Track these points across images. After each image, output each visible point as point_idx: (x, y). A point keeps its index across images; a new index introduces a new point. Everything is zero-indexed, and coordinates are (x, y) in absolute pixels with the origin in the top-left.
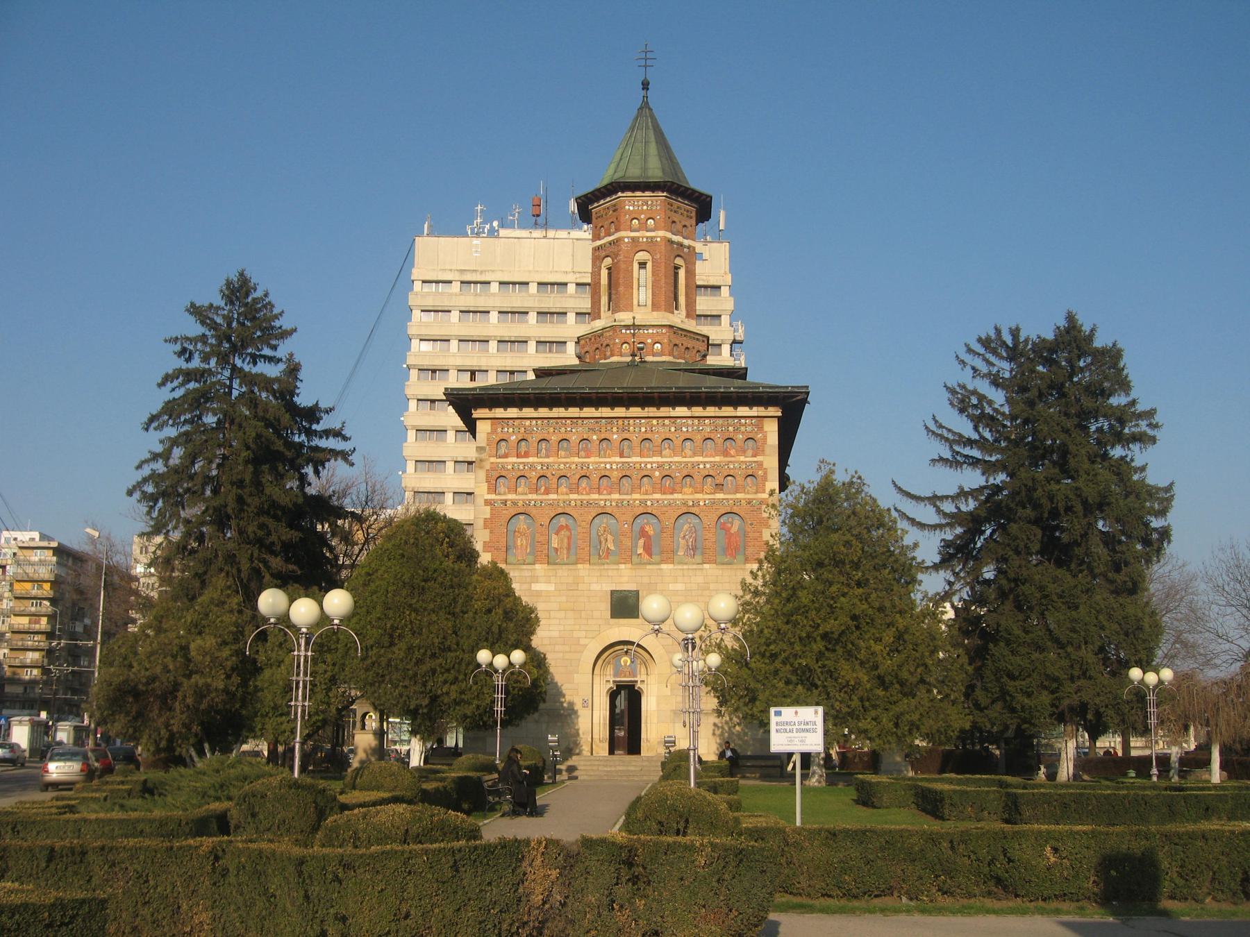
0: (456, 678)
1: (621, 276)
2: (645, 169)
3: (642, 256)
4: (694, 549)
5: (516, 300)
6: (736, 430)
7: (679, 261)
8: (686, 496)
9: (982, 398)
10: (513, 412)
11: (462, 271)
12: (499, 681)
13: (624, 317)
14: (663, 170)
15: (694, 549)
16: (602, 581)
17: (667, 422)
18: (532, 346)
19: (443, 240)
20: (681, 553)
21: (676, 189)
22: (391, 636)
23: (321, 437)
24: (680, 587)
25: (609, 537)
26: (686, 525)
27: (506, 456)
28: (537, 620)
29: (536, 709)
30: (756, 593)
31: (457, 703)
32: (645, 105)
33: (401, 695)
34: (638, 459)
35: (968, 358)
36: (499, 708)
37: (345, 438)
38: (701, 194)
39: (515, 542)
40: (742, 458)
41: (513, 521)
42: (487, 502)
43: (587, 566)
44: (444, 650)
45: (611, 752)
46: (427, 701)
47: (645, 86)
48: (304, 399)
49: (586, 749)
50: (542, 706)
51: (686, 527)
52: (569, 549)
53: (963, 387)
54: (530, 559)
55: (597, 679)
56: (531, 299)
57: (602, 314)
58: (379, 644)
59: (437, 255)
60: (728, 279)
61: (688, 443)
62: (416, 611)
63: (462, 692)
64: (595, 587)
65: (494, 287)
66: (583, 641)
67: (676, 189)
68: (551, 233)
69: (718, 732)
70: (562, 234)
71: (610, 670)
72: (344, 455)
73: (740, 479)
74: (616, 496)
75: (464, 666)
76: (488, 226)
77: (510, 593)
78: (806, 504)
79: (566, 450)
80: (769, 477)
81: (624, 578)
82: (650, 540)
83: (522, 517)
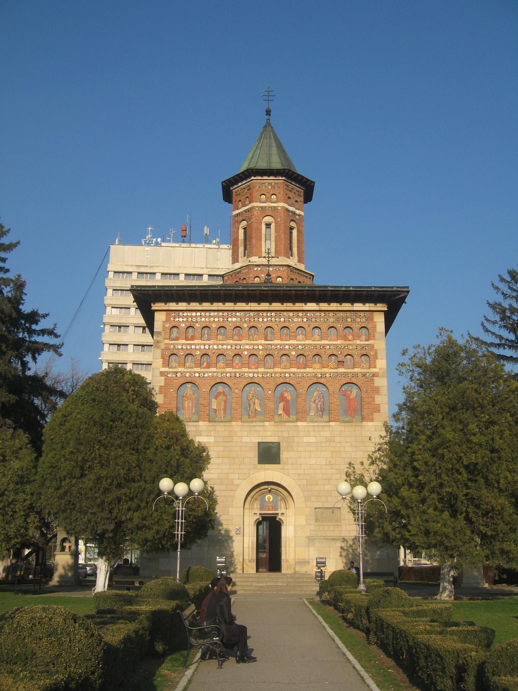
0: (139, 507)
1: (254, 232)
2: (269, 162)
3: (268, 219)
4: (322, 410)
6: (353, 321)
7: (293, 224)
8: (315, 370)
10: (183, 306)
11: (138, 266)
12: (180, 507)
13: (255, 260)
14: (282, 164)
15: (322, 410)
17: (300, 314)
20: (312, 413)
21: (290, 175)
22: (82, 468)
23: (39, 335)
24: (312, 439)
25: (257, 401)
26: (317, 392)
27: (177, 339)
28: (208, 458)
29: (205, 535)
31: (139, 528)
32: (268, 125)
33: (89, 521)
34: (279, 342)
36: (179, 532)
37: (57, 336)
38: (308, 180)
39: (183, 405)
40: (358, 342)
41: (182, 388)
42: (162, 374)
43: (240, 423)
44: (129, 481)
45: (257, 571)
46: (112, 527)
47: (268, 112)
48: (26, 308)
49: (239, 567)
50: (210, 532)
51: (316, 394)
52: (225, 410)
54: (195, 417)
55: (247, 511)
57: (240, 259)
58: (71, 475)
61: (317, 331)
62: (105, 446)
63: (144, 519)
64: (245, 439)
66: (236, 482)
67: (290, 175)
68: (193, 245)
69: (344, 554)
72: (55, 348)
74: (262, 370)
75: (145, 495)
76: (155, 240)
77: (184, 434)
78: (433, 361)
79: (223, 335)
80: (379, 355)
81: (269, 432)
82: (289, 403)
83: (189, 385)
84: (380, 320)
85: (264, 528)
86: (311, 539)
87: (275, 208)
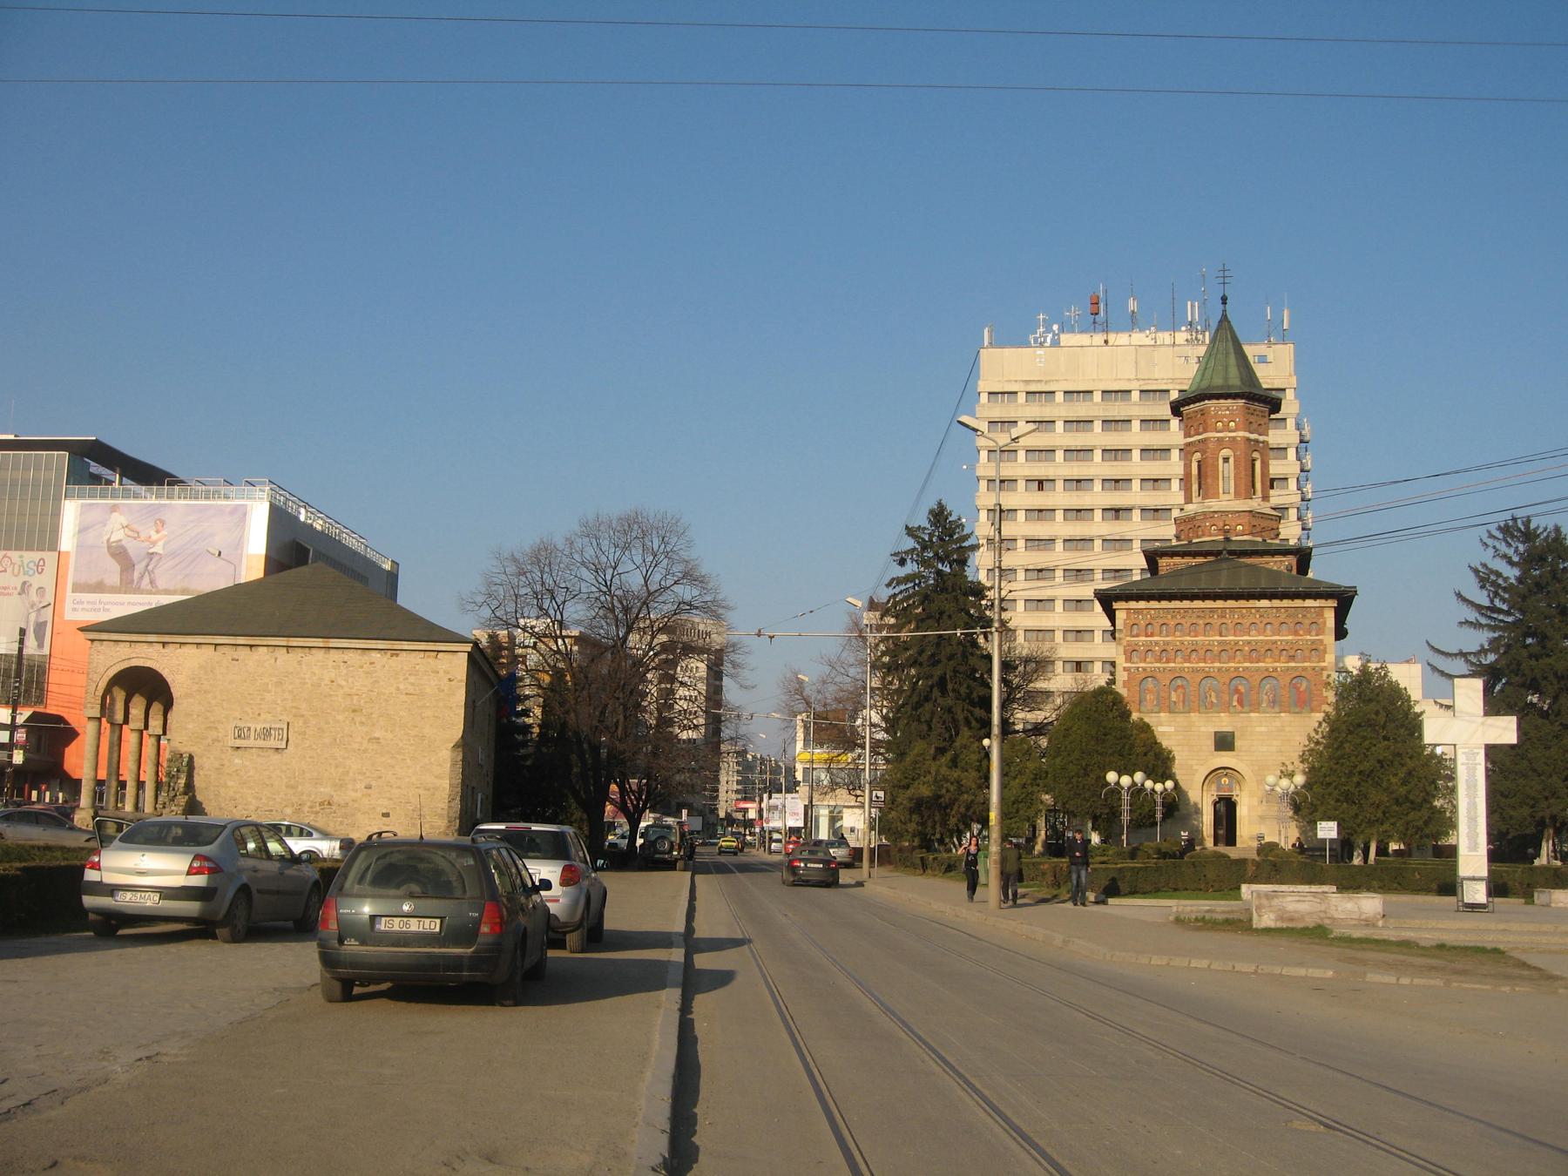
2: (1226, 379)
3: (1225, 452)
5: (1080, 410)
7: (1256, 455)
9: (1499, 574)
10: (1142, 604)
11: (1027, 382)
12: (1159, 800)
13: (1214, 505)
16: (1208, 725)
18: (1098, 455)
19: (1007, 351)
30: (1318, 743)
32: (1224, 318)
35: (1490, 542)
36: (1159, 816)
42: (1125, 669)
47: (1224, 300)
53: (1484, 565)
56: (1095, 408)
59: (1003, 366)
60: (1294, 381)
65: (1059, 397)
68: (1112, 337)
71: (1214, 787)
73: (1307, 653)
81: (1224, 723)
82: (1242, 697)
84: (1330, 618)
85: (1223, 809)
86: (1262, 818)
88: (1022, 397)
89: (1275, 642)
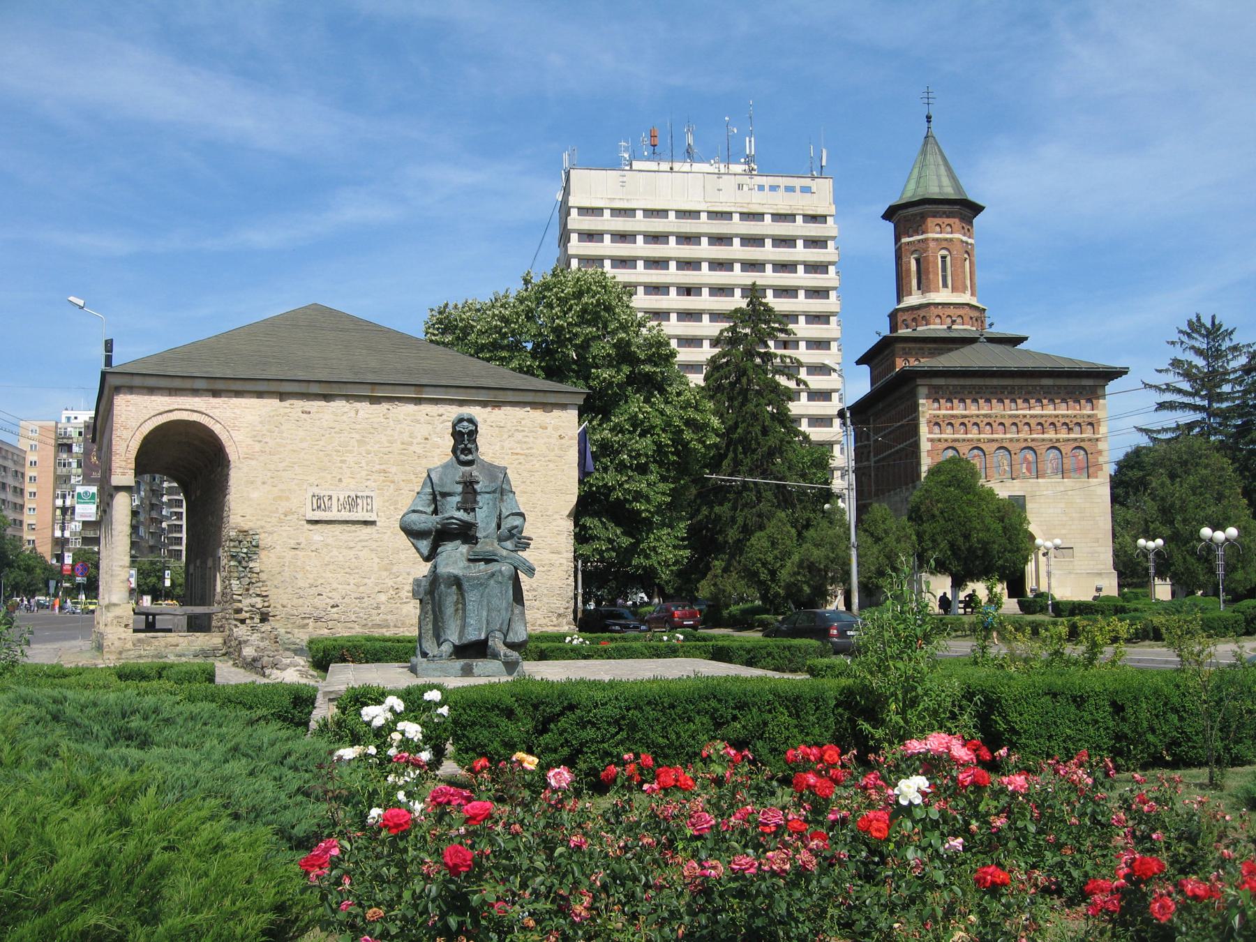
2: (940, 186)
3: (944, 252)
5: (657, 225)
8: (1051, 435)
47: (929, 118)
68: (677, 166)
70: (686, 167)
87: (951, 240)
88: (607, 213)
89: (1057, 416)
